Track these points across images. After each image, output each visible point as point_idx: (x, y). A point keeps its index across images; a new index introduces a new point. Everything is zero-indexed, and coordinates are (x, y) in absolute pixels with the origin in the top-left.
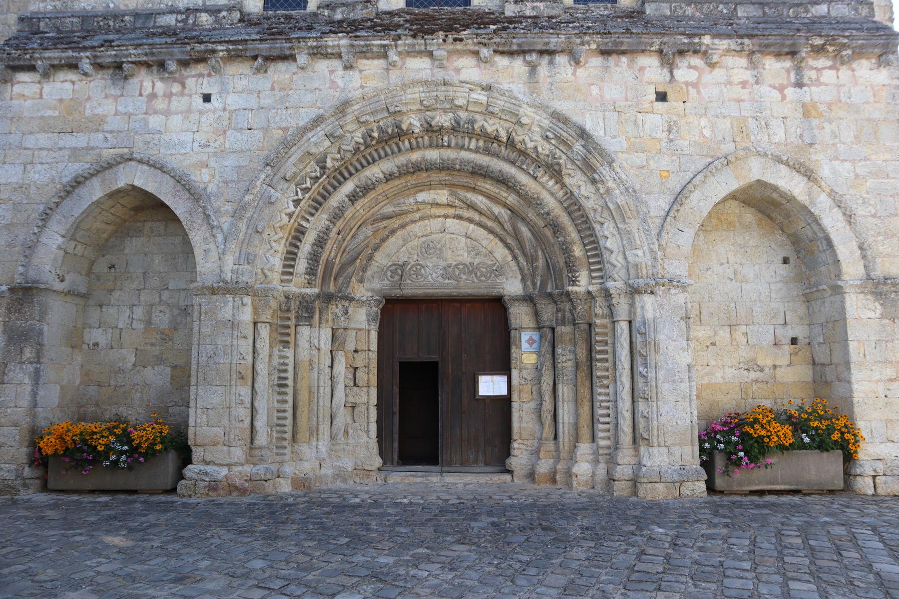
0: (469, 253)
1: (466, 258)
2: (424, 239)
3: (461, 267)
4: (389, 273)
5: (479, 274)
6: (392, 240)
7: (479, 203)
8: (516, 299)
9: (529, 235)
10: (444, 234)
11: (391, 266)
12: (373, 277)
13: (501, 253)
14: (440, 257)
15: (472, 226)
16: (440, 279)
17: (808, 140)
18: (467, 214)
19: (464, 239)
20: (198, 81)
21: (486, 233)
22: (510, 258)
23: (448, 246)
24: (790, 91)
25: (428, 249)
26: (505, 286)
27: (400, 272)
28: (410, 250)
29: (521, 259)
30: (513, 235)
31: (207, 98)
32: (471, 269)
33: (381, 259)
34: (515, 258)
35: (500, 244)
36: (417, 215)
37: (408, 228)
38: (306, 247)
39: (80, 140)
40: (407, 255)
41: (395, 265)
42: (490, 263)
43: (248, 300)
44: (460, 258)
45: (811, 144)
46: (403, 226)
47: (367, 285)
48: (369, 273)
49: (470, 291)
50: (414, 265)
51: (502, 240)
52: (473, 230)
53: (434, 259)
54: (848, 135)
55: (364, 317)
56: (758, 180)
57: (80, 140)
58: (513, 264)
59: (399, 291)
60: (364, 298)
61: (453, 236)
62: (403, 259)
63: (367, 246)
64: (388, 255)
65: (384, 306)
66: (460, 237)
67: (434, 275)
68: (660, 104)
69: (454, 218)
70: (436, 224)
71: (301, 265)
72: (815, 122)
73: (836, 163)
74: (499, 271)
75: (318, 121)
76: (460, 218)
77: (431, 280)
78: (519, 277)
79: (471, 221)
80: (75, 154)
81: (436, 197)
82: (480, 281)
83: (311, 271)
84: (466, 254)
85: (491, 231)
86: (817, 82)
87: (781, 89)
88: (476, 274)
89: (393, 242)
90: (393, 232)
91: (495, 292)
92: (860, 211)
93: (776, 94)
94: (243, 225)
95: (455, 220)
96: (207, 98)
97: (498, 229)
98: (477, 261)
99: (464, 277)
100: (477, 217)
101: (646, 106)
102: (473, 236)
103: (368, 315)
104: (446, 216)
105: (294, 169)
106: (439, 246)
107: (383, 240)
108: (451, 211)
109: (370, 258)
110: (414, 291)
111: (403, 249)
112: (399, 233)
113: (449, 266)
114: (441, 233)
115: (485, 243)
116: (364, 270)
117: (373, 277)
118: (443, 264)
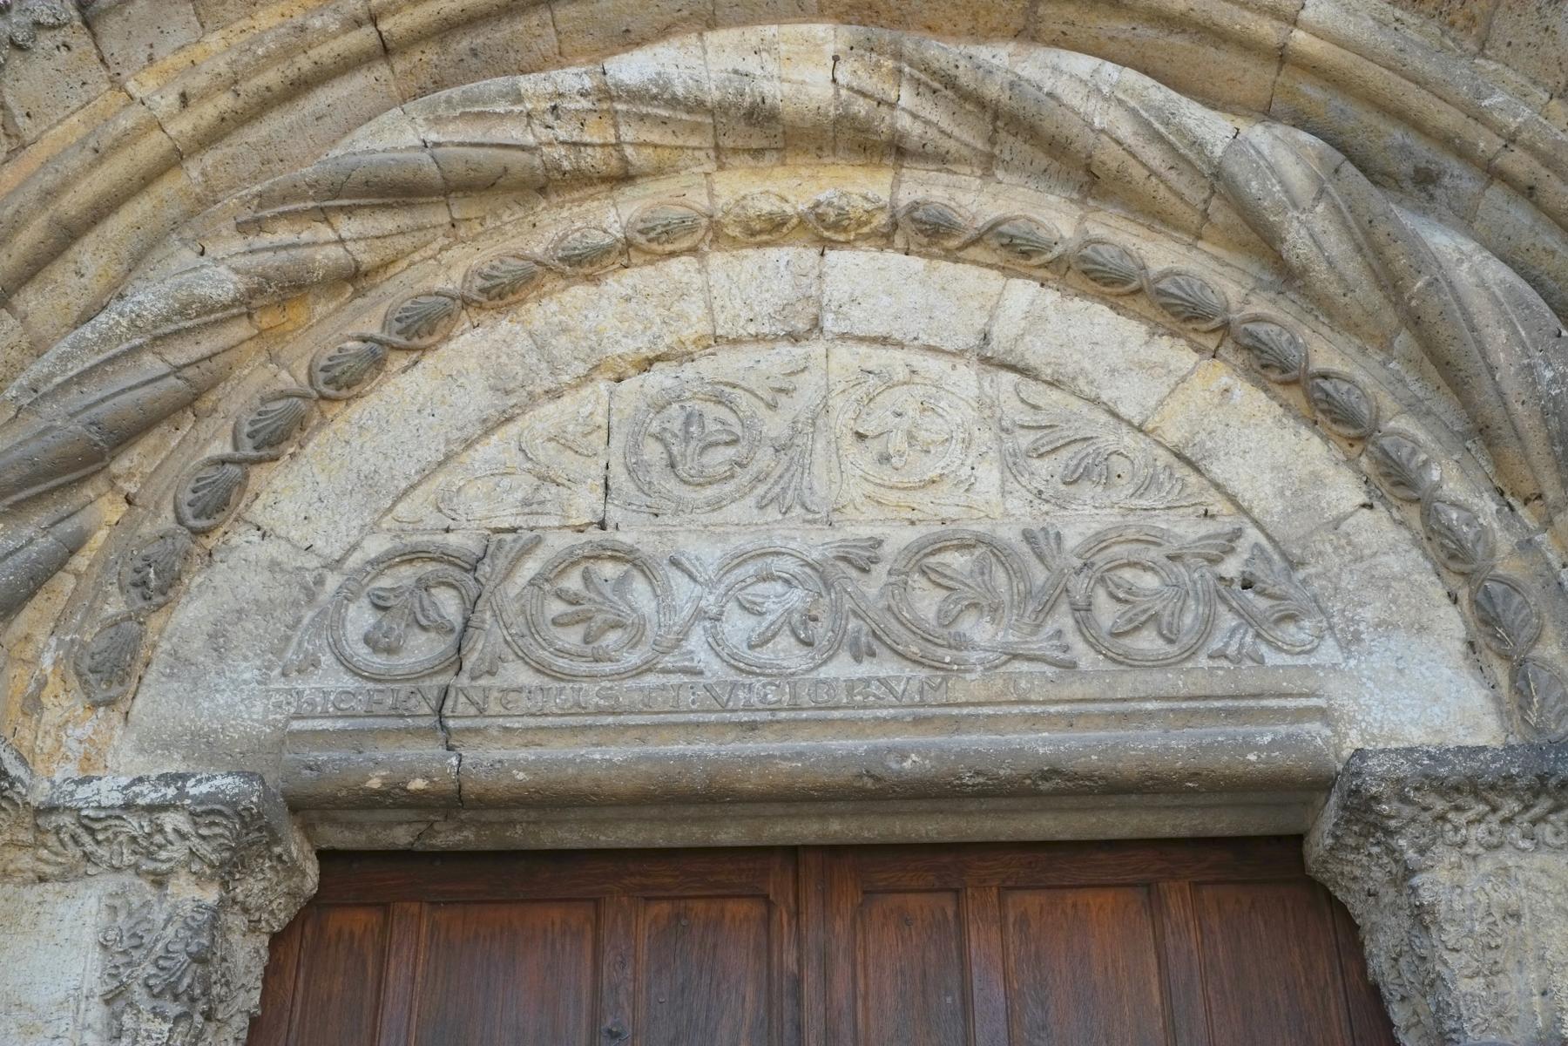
0: (1012, 465)
1: (994, 501)
2: (660, 378)
3: (957, 561)
4: (360, 617)
5: (1107, 613)
6: (407, 387)
7: (1073, 97)
8: (1457, 784)
9: (1496, 272)
10: (817, 348)
11: (384, 563)
12: (218, 641)
13: (1267, 456)
14: (781, 499)
15: (1022, 294)
16: (786, 653)
18: (975, 200)
19: (966, 378)
21: (1134, 331)
22: (1344, 491)
23: (842, 419)
25: (695, 444)
26: (1338, 693)
27: (449, 605)
28: (545, 453)
29: (1451, 479)
30: (1367, 294)
32: (1046, 582)
33: (309, 508)
34: (1395, 481)
35: (1249, 398)
36: (612, 216)
37: (541, 312)
40: (523, 485)
41: (412, 555)
42: (1188, 530)
44: (947, 504)
46: (500, 293)
47: (156, 701)
48: (192, 613)
49: (1044, 744)
50: (568, 561)
51: (1270, 366)
52: (1035, 319)
53: (734, 512)
55: (82, 969)
58: (1384, 537)
59: (431, 750)
60: (107, 791)
61: (879, 357)
62: (482, 502)
63: (188, 402)
64: (369, 483)
65: (312, 911)
66: (933, 366)
67: (738, 627)
69: (885, 238)
70: (754, 282)
74: (1267, 585)
76: (932, 233)
77: (713, 657)
78: (1452, 624)
79: (1016, 250)
81: (751, 64)
82: (1125, 661)
84: (989, 476)
85: (1183, 314)
88: (1083, 612)
89: (412, 404)
90: (421, 328)
91: (1261, 746)
95: (893, 258)
97: (1227, 283)
98: (1081, 522)
99: (980, 630)
100: (1058, 218)
102: (1035, 352)
103: (122, 948)
104: (827, 229)
106: (775, 425)
107: (343, 381)
108: (865, 187)
109: (216, 501)
110: (559, 750)
111: (493, 448)
112: (471, 345)
113: (862, 558)
114: (794, 338)
115: (1132, 396)
116: (156, 583)
117: (218, 641)
118: (817, 543)
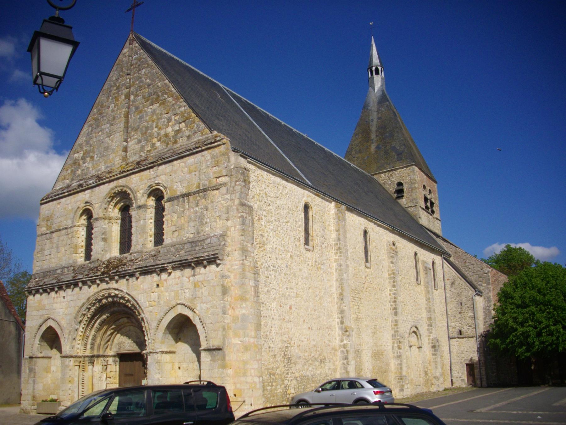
17: (194, 296)
20: (62, 293)
24: (191, 278)
31: (64, 297)
38: (90, 341)
39: (41, 312)
43: (72, 359)
45: (195, 298)
54: (206, 293)
56: (180, 314)
57: (41, 312)
68: (157, 289)
71: (89, 346)
72: (197, 289)
73: (202, 304)
75: (84, 304)
80: (41, 316)
83: (92, 348)
86: (199, 274)
87: (189, 278)
92: (207, 321)
93: (187, 280)
94: (70, 337)
96: (64, 297)
101: (153, 290)
105: (81, 319)
